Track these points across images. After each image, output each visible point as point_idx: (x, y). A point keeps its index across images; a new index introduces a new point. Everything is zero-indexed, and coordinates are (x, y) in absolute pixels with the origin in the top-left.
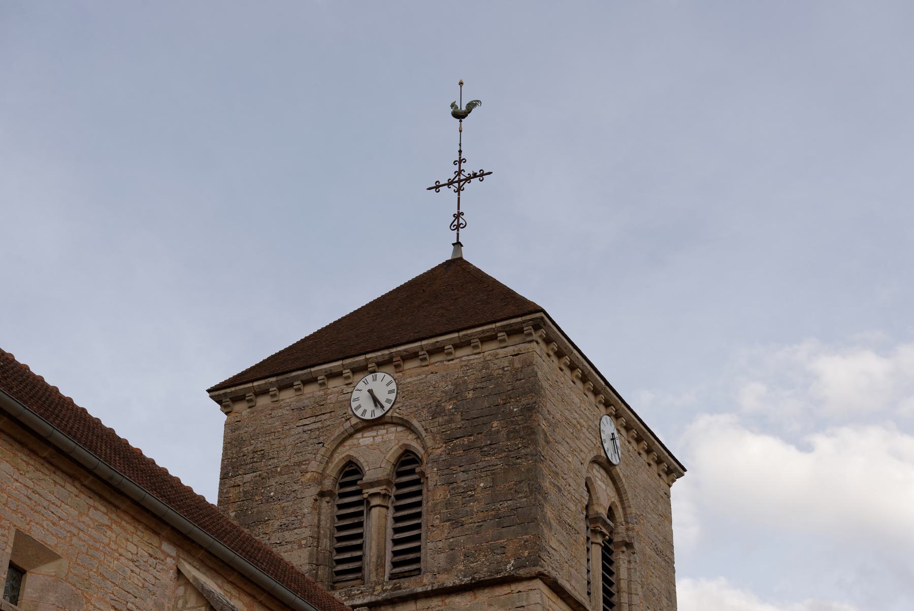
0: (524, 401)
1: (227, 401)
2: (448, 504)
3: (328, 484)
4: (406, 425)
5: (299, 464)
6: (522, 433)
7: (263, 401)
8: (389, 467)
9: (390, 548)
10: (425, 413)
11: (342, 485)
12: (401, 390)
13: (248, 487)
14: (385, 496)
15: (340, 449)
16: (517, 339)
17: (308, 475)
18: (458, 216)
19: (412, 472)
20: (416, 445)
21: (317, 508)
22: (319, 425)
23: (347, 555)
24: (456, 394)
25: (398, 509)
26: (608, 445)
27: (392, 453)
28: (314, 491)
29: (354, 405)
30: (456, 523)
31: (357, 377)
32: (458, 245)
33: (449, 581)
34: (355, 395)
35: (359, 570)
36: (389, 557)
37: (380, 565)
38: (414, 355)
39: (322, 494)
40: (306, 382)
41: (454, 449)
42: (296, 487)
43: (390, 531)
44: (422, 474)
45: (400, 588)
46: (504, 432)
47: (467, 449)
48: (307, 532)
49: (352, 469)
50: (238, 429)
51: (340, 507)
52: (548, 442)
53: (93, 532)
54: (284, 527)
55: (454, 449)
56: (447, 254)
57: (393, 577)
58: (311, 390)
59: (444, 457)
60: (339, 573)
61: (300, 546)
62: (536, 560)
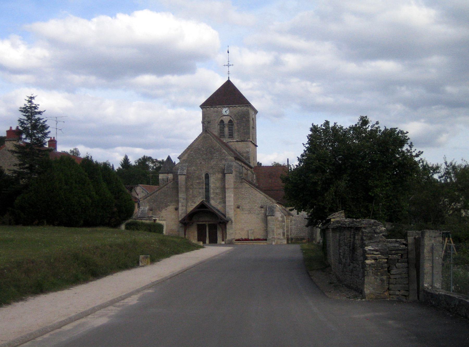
4: (231, 117)
5: (215, 120)
7: (208, 109)
10: (233, 116)
14: (227, 126)
16: (247, 107)
17: (216, 122)
18: (229, 72)
20: (232, 119)
25: (229, 128)
27: (229, 120)
29: (223, 112)
31: (223, 108)
32: (229, 77)
34: (223, 111)
36: (228, 135)
37: (227, 136)
38: (232, 106)
40: (215, 107)
49: (222, 121)
54: (213, 129)
56: (227, 79)
58: (215, 108)
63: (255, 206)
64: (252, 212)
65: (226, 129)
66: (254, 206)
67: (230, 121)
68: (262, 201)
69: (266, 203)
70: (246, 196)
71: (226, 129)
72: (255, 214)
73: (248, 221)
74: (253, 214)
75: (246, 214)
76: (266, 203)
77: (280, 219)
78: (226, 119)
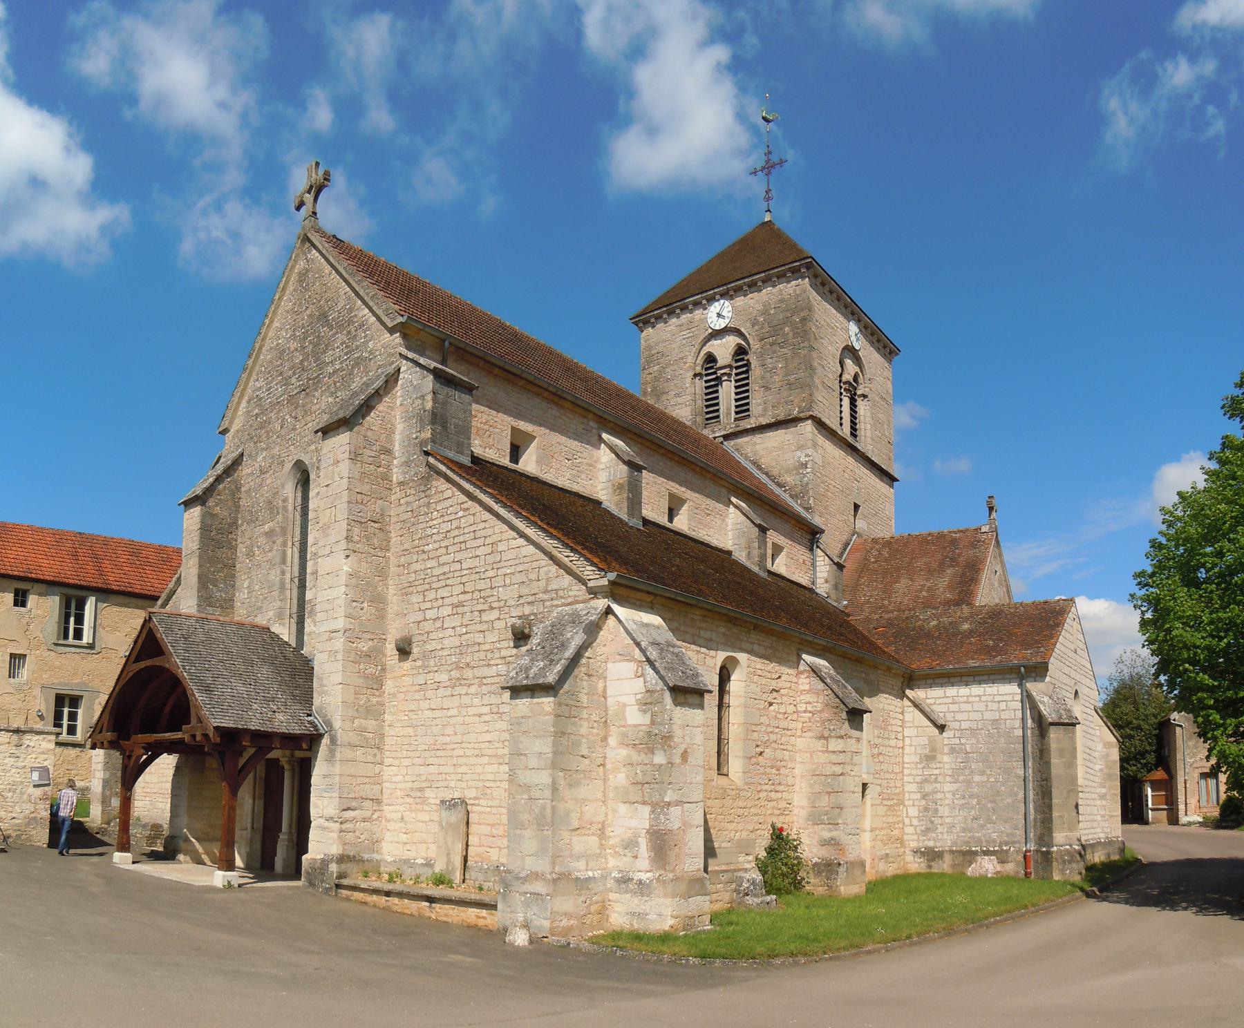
0: (802, 314)
1: (641, 325)
2: (762, 378)
3: (698, 369)
4: (737, 332)
5: (682, 358)
6: (801, 334)
8: (731, 357)
9: (733, 403)
10: (748, 324)
11: (706, 369)
12: (735, 311)
13: (656, 374)
15: (704, 348)
17: (688, 365)
19: (742, 359)
21: (693, 384)
22: (692, 334)
23: (711, 409)
24: (765, 312)
26: (853, 339)
28: (691, 374)
29: (709, 321)
30: (767, 388)
33: (764, 421)
35: (718, 417)
36: (733, 409)
37: (728, 414)
39: (695, 375)
41: (764, 345)
42: (681, 372)
43: (733, 394)
44: (748, 360)
45: (739, 426)
46: (791, 334)
47: (772, 344)
48: (689, 398)
50: (648, 340)
51: (706, 382)
52: (816, 339)
53: (551, 421)
54: (677, 395)
55: (764, 345)
57: (736, 419)
59: (759, 350)
60: (707, 419)
61: (686, 406)
62: (810, 408)
63: (484, 627)
64: (468, 673)
65: (727, 391)
66: (479, 627)
67: (741, 352)
68: (525, 591)
69: (545, 597)
70: (446, 569)
71: (727, 391)
72: (485, 689)
73: (447, 739)
74: (473, 689)
75: (441, 692)
76: (545, 597)
77: (636, 718)
78: (723, 350)
